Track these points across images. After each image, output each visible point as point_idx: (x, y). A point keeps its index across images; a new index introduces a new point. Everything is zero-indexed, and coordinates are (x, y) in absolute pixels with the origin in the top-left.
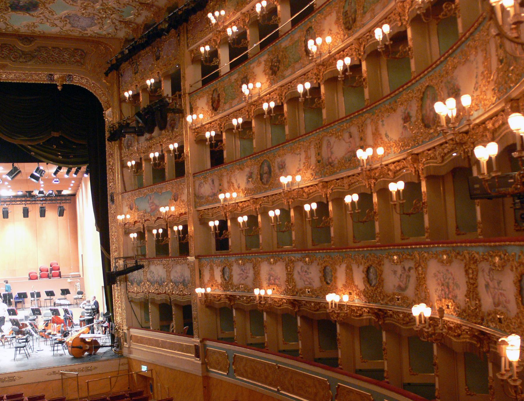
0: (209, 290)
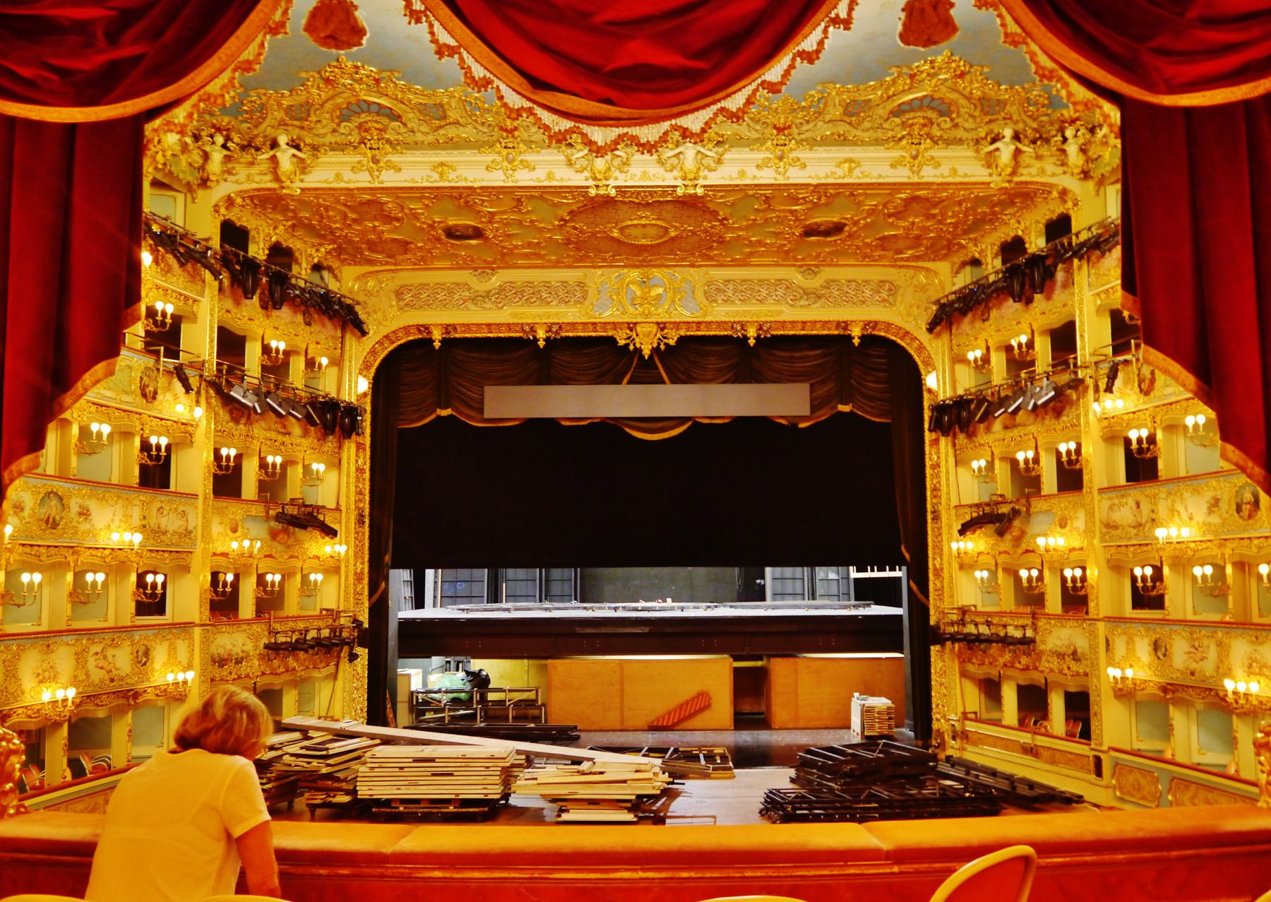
0: (1129, 673)
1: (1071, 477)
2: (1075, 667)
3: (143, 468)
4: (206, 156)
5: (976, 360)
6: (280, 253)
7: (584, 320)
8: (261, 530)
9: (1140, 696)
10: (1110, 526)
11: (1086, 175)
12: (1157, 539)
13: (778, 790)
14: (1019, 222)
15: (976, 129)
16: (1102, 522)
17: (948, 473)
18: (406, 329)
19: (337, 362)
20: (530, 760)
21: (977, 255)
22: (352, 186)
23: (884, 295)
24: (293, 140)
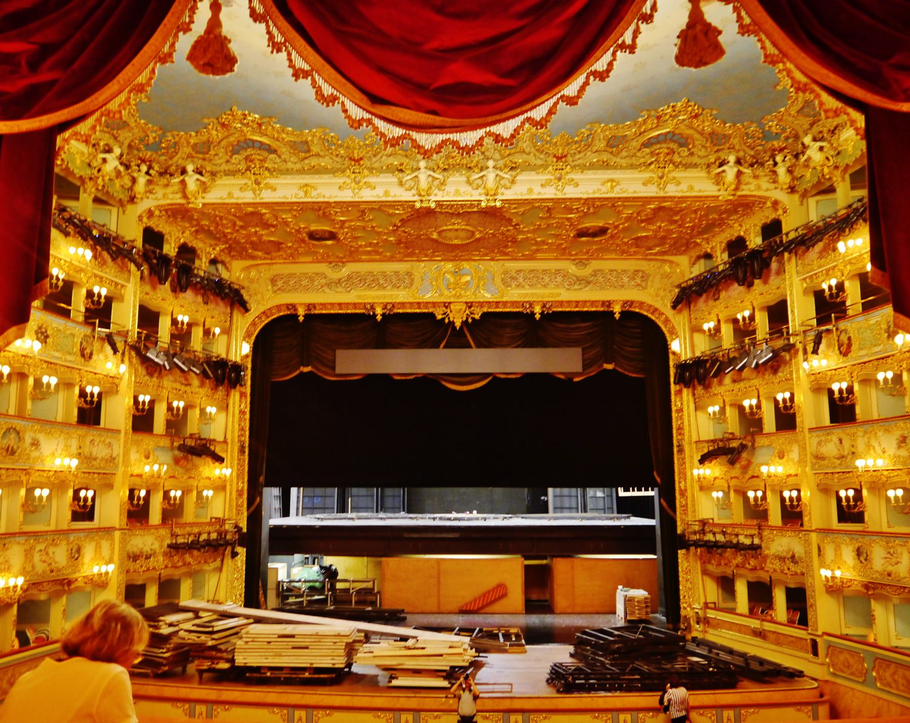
0: (838, 573)
1: (786, 419)
2: (793, 568)
3: (80, 410)
4: (134, 180)
5: (709, 330)
6: (186, 251)
7: (411, 300)
8: (167, 457)
9: (847, 591)
10: (818, 457)
11: (792, 189)
12: (857, 468)
13: (561, 664)
14: (741, 225)
15: (707, 156)
16: (812, 454)
17: (689, 416)
18: (279, 307)
19: (227, 332)
20: (367, 637)
21: (709, 250)
22: (240, 201)
23: (638, 281)
24: (197, 169)
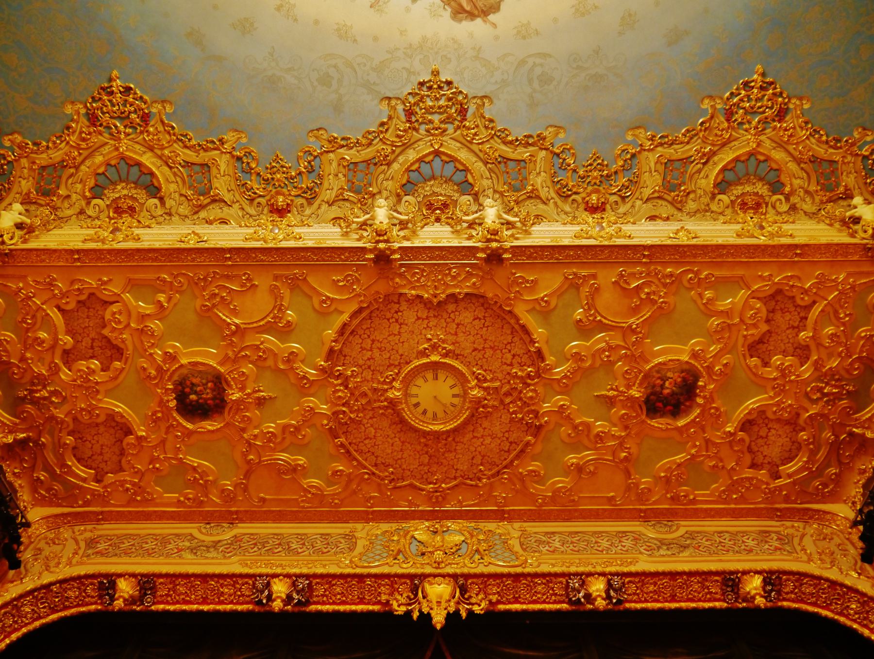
23: (776, 544)
